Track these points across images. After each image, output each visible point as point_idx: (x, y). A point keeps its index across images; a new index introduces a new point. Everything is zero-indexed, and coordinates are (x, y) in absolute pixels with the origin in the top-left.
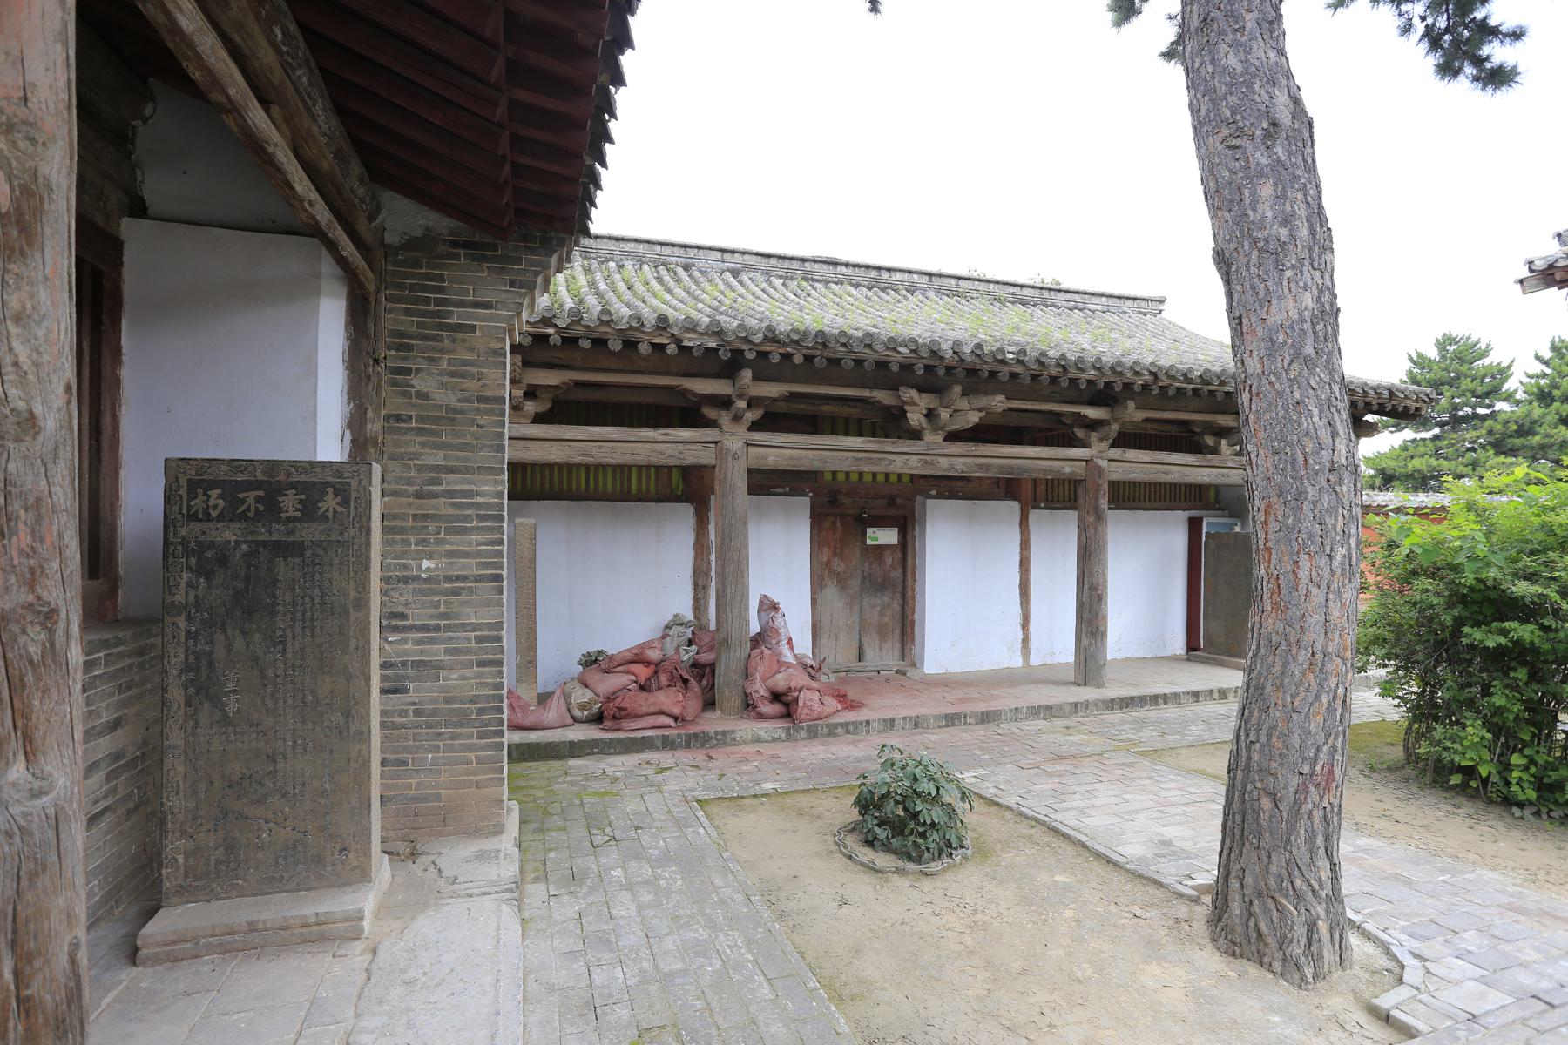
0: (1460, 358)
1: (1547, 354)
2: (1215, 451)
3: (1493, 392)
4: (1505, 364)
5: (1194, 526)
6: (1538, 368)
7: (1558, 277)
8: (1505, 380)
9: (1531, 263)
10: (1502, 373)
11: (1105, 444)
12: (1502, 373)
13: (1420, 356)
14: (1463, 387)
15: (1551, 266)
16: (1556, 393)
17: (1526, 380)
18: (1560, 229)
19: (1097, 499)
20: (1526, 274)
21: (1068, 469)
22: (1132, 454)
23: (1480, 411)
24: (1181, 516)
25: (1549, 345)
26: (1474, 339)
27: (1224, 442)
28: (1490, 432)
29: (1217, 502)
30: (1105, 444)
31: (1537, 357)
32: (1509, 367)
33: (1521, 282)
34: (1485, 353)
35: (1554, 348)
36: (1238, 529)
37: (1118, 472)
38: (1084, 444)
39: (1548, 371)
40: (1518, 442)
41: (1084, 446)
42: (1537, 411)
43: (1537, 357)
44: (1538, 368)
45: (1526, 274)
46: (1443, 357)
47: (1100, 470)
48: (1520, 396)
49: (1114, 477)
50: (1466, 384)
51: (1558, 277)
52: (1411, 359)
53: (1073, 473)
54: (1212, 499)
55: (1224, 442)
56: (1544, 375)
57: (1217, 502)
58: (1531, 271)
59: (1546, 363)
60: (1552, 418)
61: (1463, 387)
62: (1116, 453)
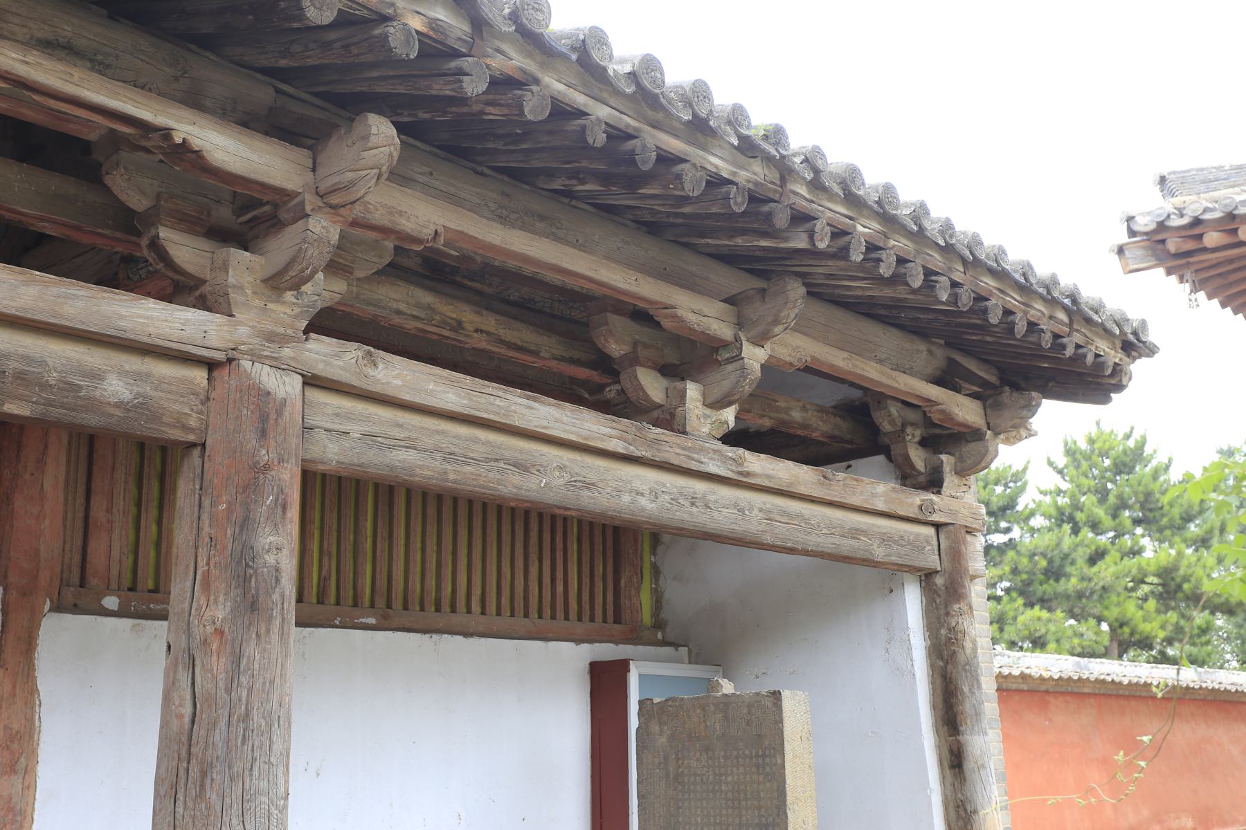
1: (1061, 461)
2: (670, 419)
5: (606, 684)
7: (1172, 245)
8: (1022, 490)
9: (1130, 219)
11: (289, 312)
15: (1162, 226)
16: (1079, 516)
19: (246, 523)
20: (1124, 238)
21: (117, 384)
22: (396, 374)
24: (569, 660)
25: (1061, 448)
27: (693, 391)
28: (1015, 571)
29: (659, 624)
30: (289, 312)
31: (1050, 463)
32: (1024, 470)
33: (1121, 251)
35: (1070, 452)
36: (727, 687)
37: (348, 436)
38: (180, 288)
39: (1065, 486)
40: (1049, 588)
41: (203, 303)
42: (1068, 542)
43: (1050, 463)
45: (1124, 238)
47: (266, 411)
48: (1038, 522)
49: (332, 453)
53: (141, 407)
54: (647, 618)
55: (693, 391)
56: (1059, 492)
57: (659, 624)
58: (1132, 233)
59: (1060, 472)
62: (330, 355)
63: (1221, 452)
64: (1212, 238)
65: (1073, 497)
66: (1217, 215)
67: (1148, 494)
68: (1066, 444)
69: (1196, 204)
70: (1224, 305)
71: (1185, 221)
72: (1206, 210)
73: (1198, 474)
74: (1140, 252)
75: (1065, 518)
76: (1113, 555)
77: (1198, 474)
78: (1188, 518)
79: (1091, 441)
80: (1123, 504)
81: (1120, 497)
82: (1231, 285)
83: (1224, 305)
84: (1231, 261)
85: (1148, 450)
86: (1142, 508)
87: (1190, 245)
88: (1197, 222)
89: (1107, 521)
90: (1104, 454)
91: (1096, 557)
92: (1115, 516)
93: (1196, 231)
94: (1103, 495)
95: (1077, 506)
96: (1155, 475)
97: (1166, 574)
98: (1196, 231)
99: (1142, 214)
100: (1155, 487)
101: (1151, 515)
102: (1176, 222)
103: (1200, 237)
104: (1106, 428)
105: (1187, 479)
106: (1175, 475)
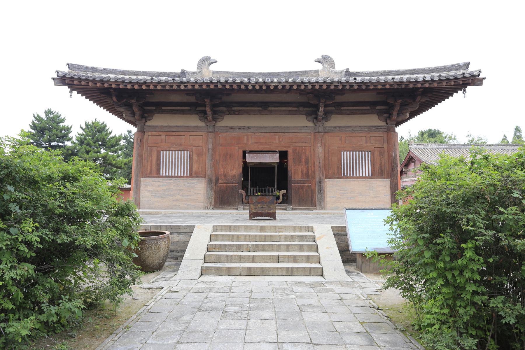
0: (53, 119)
1: (84, 127)
3: (65, 137)
4: (69, 127)
6: (81, 132)
9: (58, 72)
10: (68, 129)
12: (68, 129)
13: (38, 116)
14: (53, 132)
15: (64, 76)
16: (86, 142)
17: (77, 135)
18: (69, 62)
23: (61, 144)
25: (84, 124)
26: (59, 114)
31: (81, 127)
32: (71, 128)
33: (53, 79)
34: (63, 121)
35: (86, 125)
39: (84, 133)
43: (81, 127)
44: (81, 132)
46: (47, 118)
50: (54, 131)
51: (67, 81)
52: (34, 116)
59: (83, 130)
60: (83, 150)
61: (53, 132)
63: (128, 131)
64: (83, 83)
65: (85, 137)
66: (76, 77)
67: (104, 139)
68: (86, 123)
69: (74, 73)
70: (86, 98)
71: (69, 76)
72: (75, 75)
73: (117, 136)
74: (58, 81)
75: (81, 142)
76: (92, 152)
77: (117, 136)
78: (113, 146)
79: (93, 123)
80: (97, 140)
81: (97, 138)
82: (88, 94)
83: (86, 98)
84: (85, 88)
85: (107, 128)
86: (102, 142)
87: (71, 83)
88: (72, 78)
89: (92, 144)
90: (95, 127)
91: (88, 152)
92: (95, 143)
93: (72, 80)
94: (93, 136)
95: (85, 139)
96: (106, 135)
97: (104, 158)
98: (72, 80)
99: (61, 72)
100: (106, 137)
101: (104, 144)
102: (68, 76)
103: (73, 81)
104: (98, 120)
105: (115, 137)
106: (112, 135)
